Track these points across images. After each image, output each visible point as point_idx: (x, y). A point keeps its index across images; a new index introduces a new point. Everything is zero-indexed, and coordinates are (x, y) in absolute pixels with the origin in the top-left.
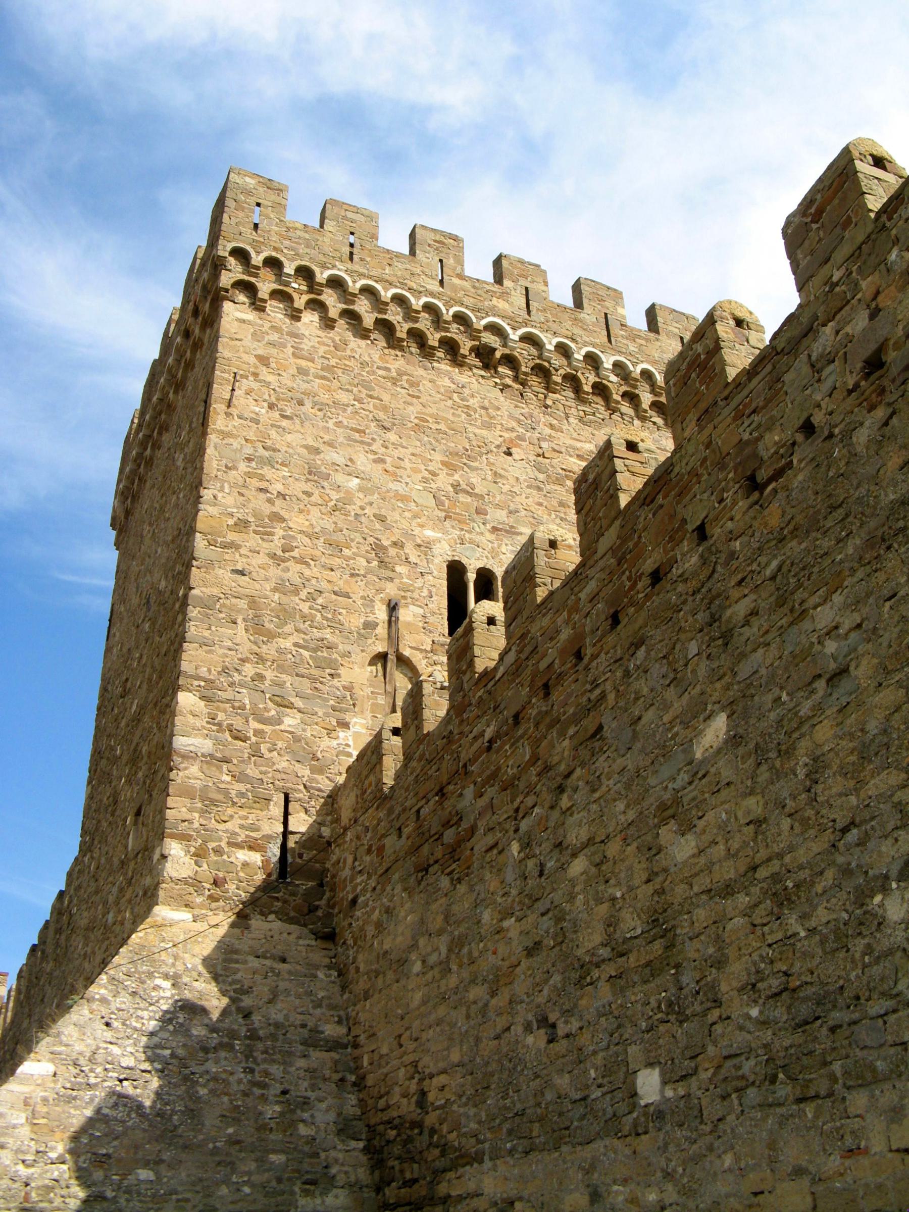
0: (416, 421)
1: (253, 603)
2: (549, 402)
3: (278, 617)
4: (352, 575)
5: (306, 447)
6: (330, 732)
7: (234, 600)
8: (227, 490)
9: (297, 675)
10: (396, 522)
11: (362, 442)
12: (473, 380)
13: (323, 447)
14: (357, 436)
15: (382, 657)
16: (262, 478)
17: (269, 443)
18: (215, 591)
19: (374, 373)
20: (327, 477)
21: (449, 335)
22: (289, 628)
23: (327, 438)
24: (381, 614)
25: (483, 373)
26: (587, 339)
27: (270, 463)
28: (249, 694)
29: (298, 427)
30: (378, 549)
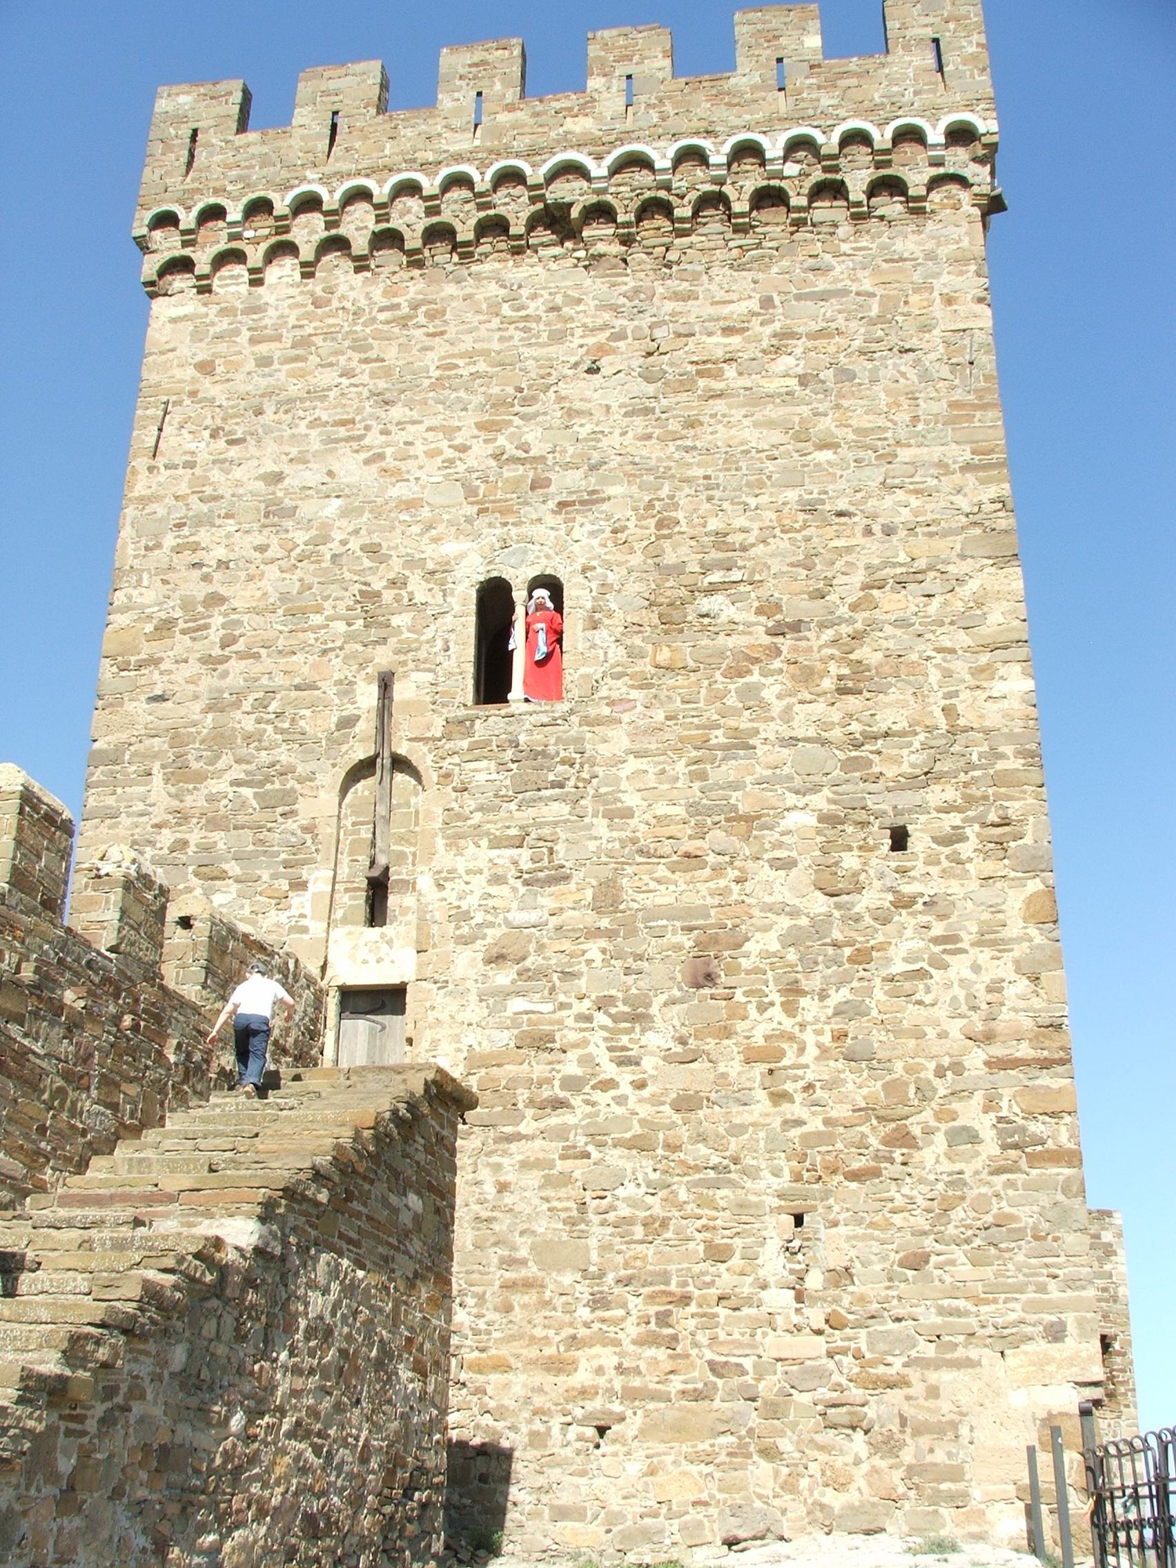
0: (438, 373)
2: (672, 256)
3: (210, 748)
4: (325, 652)
6: (281, 900)
7: (148, 742)
8: (145, 583)
10: (396, 547)
11: (349, 439)
13: (287, 469)
14: (342, 432)
16: (195, 548)
17: (208, 490)
18: (123, 737)
23: (294, 452)
24: (368, 696)
27: (200, 521)
30: (370, 596)
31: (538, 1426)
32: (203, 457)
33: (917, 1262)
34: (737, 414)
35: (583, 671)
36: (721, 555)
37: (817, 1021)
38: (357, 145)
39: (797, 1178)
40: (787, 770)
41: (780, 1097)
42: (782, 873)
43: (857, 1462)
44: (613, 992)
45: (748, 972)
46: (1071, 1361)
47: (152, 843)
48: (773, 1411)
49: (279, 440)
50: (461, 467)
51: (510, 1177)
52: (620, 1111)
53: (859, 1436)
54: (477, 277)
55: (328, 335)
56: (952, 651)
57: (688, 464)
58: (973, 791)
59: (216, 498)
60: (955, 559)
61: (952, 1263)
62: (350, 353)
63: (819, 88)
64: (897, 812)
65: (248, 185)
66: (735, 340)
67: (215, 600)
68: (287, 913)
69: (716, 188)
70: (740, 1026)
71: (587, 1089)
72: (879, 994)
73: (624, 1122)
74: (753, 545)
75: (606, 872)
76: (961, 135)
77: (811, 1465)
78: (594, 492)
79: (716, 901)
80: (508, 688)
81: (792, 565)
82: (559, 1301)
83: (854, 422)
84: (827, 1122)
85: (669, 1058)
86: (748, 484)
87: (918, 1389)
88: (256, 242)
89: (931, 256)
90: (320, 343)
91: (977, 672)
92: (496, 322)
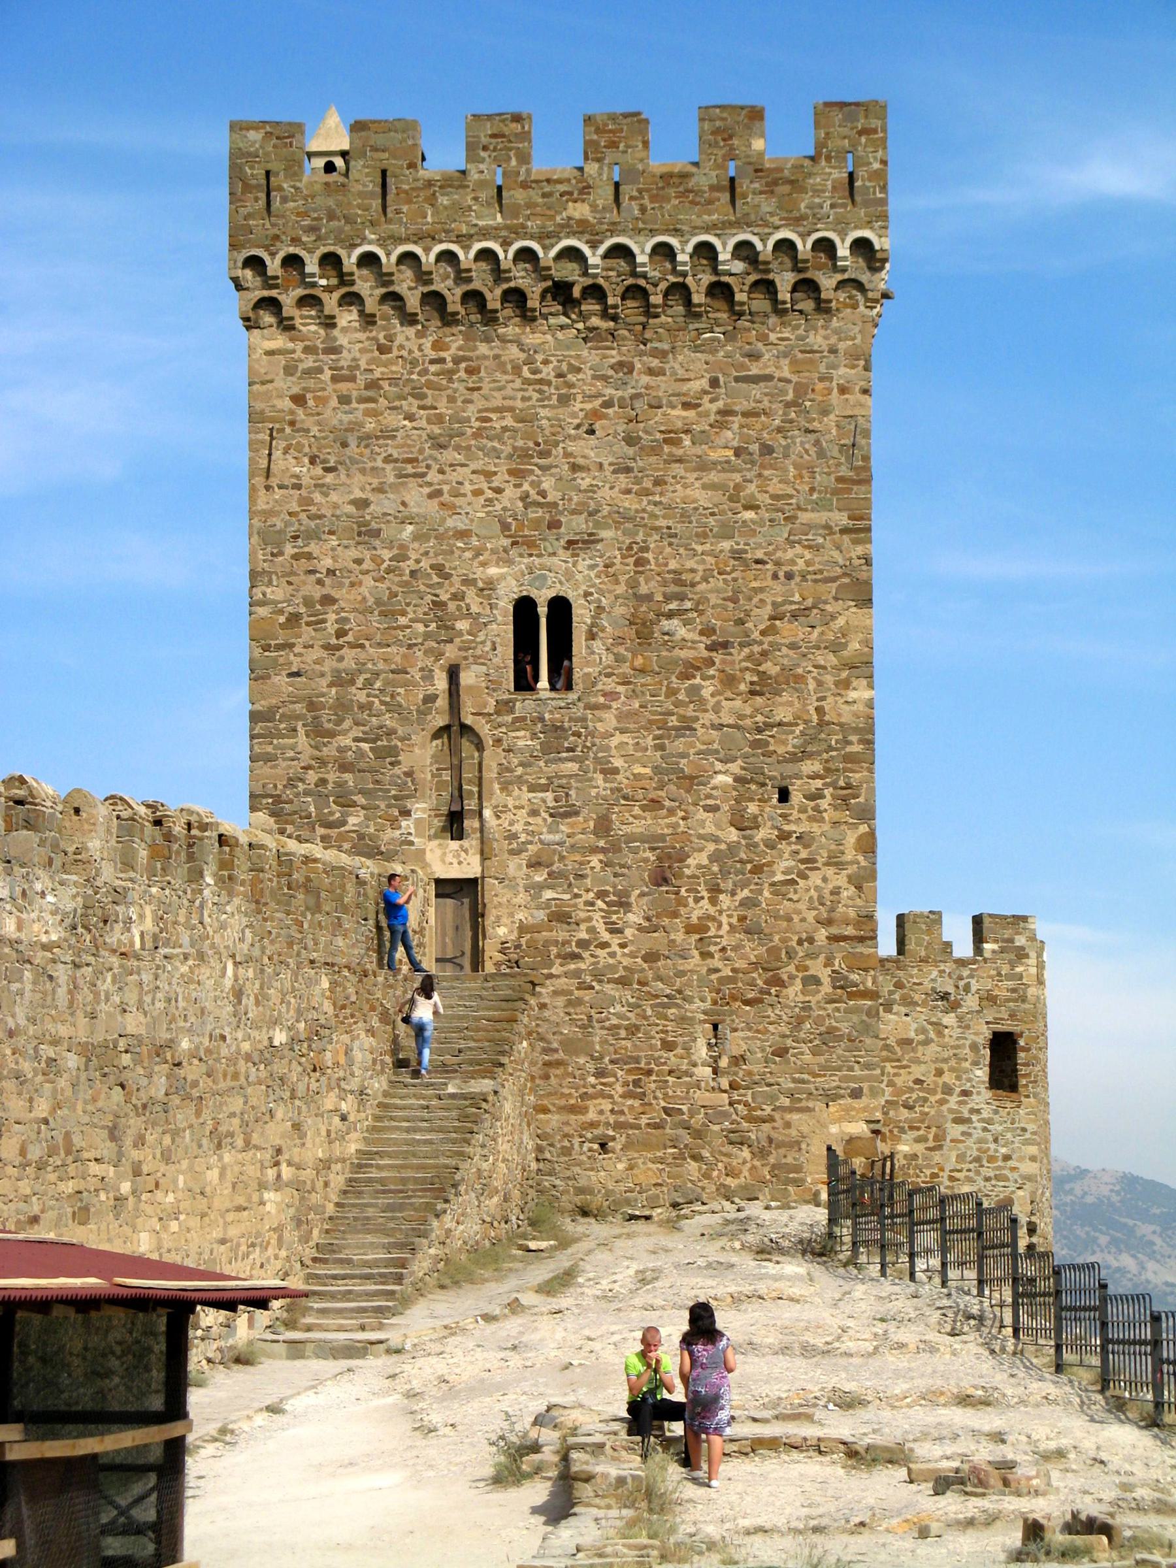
0: (477, 424)
1: (312, 706)
4: (410, 646)
6: (394, 823)
11: (415, 475)
12: (549, 337)
13: (372, 497)
14: (410, 469)
15: (447, 728)
16: (309, 556)
17: (313, 509)
19: (425, 372)
20: (377, 533)
21: (512, 284)
22: (347, 724)
23: (375, 482)
24: (441, 683)
25: (563, 320)
26: (699, 223)
29: (343, 477)
30: (438, 605)
31: (566, 1144)
32: (306, 481)
33: (781, 1052)
35: (586, 670)
36: (677, 589)
37: (729, 909)
38: (405, 208)
39: (715, 1003)
40: (716, 746)
41: (705, 955)
43: (745, 1162)
46: (865, 1109)
47: (301, 780)
48: (698, 1134)
49: (363, 471)
50: (498, 507)
51: (547, 1001)
52: (611, 961)
53: (745, 1148)
54: (503, 340)
55: (393, 381)
56: (824, 668)
57: (656, 517)
58: (831, 765)
61: (802, 1053)
63: (761, 193)
64: (783, 778)
65: (319, 238)
66: (691, 414)
67: (328, 600)
68: (398, 832)
69: (680, 279)
70: (682, 911)
72: (766, 894)
73: (613, 968)
75: (602, 810)
76: (862, 246)
78: (591, 534)
79: (670, 831)
80: (536, 678)
82: (578, 1073)
83: (770, 489)
84: (734, 970)
85: (640, 929)
86: (697, 535)
87: (779, 1123)
88: (329, 289)
89: (833, 351)
90: (387, 388)
91: (837, 684)
92: (518, 381)
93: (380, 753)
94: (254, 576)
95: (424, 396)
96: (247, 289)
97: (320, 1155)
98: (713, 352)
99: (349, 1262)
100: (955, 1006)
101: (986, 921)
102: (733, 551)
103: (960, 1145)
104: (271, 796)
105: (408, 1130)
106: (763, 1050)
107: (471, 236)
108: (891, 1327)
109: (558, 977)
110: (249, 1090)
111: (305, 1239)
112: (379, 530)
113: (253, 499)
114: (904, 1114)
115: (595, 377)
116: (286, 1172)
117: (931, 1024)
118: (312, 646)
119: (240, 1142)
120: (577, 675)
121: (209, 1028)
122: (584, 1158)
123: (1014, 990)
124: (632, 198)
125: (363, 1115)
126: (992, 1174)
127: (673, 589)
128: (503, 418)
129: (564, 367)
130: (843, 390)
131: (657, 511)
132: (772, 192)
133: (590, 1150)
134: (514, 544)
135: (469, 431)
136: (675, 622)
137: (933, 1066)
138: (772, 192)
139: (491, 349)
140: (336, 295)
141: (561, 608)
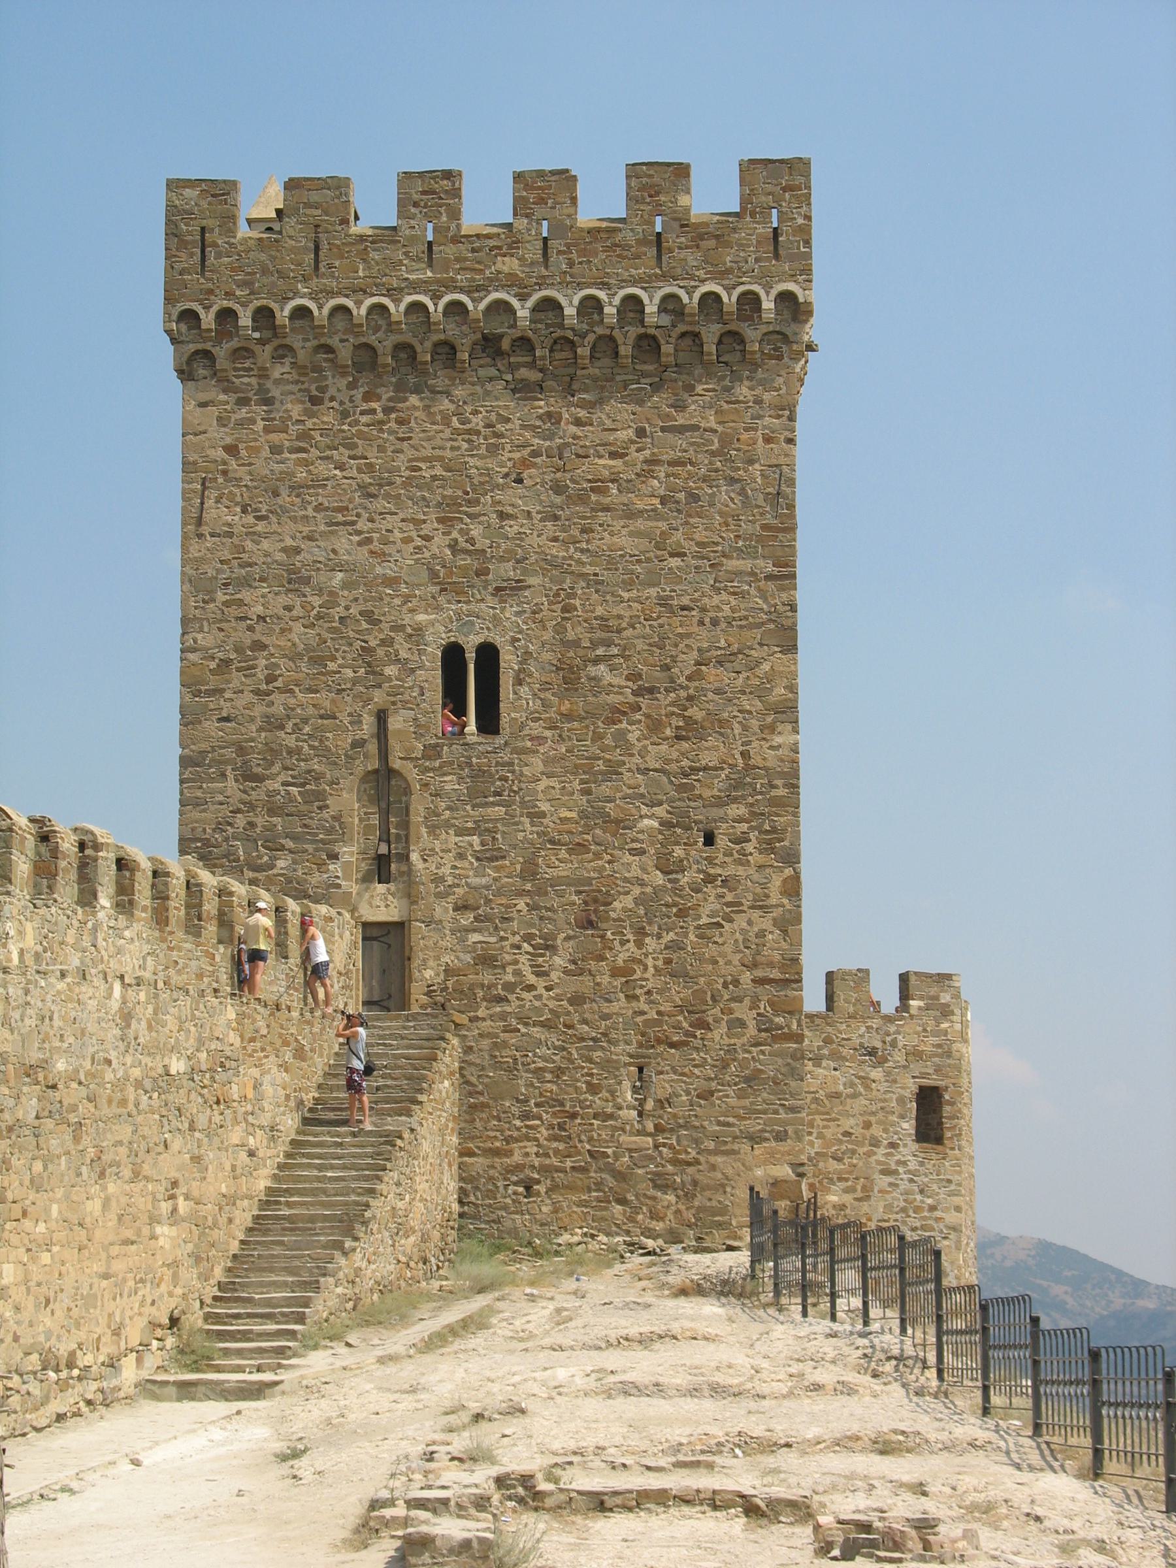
0: (407, 473)
1: (241, 750)
4: (339, 692)
5: (284, 550)
6: (321, 866)
8: (206, 629)
9: (287, 815)
11: (345, 524)
14: (340, 518)
15: (376, 771)
16: (241, 603)
18: (204, 746)
19: (357, 422)
20: (307, 581)
22: (276, 768)
23: (306, 530)
25: (493, 372)
28: (243, 845)
33: (707, 1095)
34: (618, 524)
35: (513, 715)
36: (604, 635)
38: (337, 264)
39: (640, 1045)
40: (642, 790)
42: (637, 858)
44: (534, 931)
45: (614, 920)
47: (230, 824)
49: (294, 519)
50: (427, 554)
52: (537, 1004)
55: (324, 432)
56: (750, 712)
57: (583, 564)
59: (250, 565)
60: (757, 646)
61: (727, 1096)
62: (341, 449)
65: (252, 293)
67: (259, 646)
69: (608, 332)
71: (518, 990)
72: (692, 937)
74: (625, 629)
76: (786, 298)
77: (644, 1208)
78: (518, 581)
81: (650, 645)
84: (659, 1013)
85: (566, 972)
86: (623, 581)
88: (262, 342)
89: (758, 401)
91: (762, 728)
92: (448, 431)
93: (307, 800)
94: (185, 621)
95: (355, 446)
96: (182, 342)
97: (224, 1190)
98: (641, 403)
99: (249, 1300)
100: (882, 1061)
101: (913, 979)
102: (659, 598)
103: (888, 1196)
104: (199, 840)
105: (320, 1168)
106: (688, 1093)
107: (402, 289)
108: (807, 1367)
109: (484, 1019)
110: (140, 1119)
111: (205, 1277)
112: (310, 577)
113: (185, 548)
114: (833, 1165)
115: (523, 427)
116: (183, 1206)
117: (860, 1078)
118: (242, 692)
119: (127, 1173)
120: (504, 720)
121: (92, 1050)
122: (508, 1201)
123: (939, 1046)
124: (559, 252)
125: (274, 1152)
126: (918, 1224)
127: (599, 634)
128: (433, 467)
129: (493, 416)
130: (768, 440)
131: (584, 558)
132: (698, 247)
133: (515, 1193)
134: (442, 590)
135: (398, 480)
136: (602, 667)
137: (861, 1119)
138: (698, 247)
139: (422, 399)
140: (268, 348)
141: (488, 655)
